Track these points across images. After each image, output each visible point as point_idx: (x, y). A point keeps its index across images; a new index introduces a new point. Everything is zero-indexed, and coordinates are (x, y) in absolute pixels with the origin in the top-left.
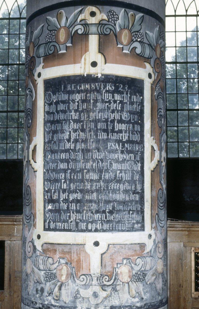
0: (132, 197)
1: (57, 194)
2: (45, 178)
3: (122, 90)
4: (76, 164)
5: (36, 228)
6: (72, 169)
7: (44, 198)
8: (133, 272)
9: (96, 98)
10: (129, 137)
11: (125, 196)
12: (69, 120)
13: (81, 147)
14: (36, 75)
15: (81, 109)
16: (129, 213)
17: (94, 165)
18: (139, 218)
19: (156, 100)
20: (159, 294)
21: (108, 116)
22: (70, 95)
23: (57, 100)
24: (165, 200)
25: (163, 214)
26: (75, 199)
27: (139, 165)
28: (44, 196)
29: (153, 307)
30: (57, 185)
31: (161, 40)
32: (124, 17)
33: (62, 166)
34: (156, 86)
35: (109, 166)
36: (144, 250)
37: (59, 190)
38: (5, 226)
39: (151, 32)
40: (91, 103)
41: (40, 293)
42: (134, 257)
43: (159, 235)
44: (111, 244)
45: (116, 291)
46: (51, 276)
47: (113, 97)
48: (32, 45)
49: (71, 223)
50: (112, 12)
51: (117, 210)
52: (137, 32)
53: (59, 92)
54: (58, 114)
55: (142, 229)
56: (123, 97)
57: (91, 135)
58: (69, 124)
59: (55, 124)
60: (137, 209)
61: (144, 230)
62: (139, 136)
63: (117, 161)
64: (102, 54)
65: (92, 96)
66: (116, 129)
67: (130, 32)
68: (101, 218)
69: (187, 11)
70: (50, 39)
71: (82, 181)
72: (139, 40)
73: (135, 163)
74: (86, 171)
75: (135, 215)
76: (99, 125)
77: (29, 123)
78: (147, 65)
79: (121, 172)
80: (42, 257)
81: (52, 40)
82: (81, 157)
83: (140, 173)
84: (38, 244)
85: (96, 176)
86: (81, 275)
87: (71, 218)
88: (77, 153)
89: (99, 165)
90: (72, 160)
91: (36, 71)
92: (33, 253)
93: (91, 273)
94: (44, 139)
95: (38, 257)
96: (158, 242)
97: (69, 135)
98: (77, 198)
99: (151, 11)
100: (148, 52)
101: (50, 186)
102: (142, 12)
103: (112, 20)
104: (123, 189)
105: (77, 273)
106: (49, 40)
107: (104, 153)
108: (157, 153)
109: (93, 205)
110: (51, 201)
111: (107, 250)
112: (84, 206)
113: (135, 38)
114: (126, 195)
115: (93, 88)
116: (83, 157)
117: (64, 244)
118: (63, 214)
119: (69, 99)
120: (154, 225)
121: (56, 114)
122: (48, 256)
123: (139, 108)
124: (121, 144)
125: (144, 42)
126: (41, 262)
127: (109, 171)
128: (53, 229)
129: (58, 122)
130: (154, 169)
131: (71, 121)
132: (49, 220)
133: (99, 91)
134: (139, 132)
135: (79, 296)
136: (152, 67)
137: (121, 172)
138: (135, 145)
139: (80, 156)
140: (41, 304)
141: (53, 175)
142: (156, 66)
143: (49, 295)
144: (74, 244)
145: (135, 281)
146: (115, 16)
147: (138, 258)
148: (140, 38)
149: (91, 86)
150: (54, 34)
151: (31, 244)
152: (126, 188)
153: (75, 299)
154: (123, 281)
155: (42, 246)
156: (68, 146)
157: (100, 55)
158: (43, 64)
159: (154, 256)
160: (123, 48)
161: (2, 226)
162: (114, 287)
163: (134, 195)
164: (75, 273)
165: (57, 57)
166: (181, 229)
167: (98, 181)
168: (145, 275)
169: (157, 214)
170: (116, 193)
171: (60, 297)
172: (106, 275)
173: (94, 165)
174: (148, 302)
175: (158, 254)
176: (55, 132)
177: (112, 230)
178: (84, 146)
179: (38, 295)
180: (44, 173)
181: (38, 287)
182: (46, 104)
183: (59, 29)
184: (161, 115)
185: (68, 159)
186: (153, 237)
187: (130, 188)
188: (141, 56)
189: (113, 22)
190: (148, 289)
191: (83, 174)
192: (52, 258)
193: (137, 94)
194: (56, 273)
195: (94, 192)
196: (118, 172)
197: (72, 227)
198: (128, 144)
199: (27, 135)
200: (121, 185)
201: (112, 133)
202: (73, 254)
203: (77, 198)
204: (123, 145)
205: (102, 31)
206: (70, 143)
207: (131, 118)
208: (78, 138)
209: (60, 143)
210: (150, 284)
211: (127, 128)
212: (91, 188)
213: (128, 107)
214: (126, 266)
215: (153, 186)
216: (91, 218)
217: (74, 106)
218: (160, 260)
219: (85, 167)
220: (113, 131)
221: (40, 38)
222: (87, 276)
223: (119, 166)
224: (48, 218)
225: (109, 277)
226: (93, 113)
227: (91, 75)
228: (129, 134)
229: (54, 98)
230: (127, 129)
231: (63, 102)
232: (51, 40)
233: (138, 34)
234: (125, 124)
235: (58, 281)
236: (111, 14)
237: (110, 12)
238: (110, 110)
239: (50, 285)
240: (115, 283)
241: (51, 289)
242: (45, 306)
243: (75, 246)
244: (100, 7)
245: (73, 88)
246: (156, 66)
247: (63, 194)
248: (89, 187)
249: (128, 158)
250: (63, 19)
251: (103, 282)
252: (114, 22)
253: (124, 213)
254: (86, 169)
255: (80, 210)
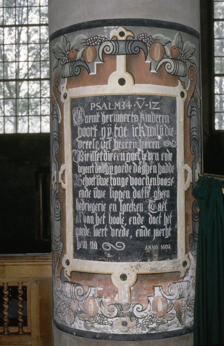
84: (68, 269)
130: (187, 189)
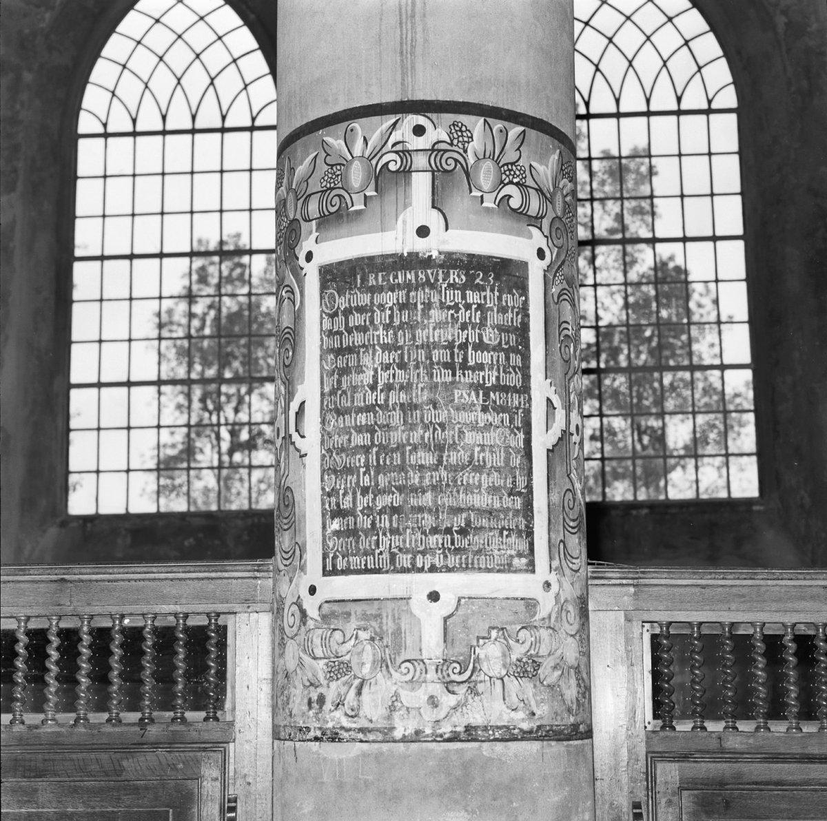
0: (508, 502)
1: (349, 498)
2: (325, 466)
3: (482, 283)
4: (390, 435)
5: (305, 574)
6: (380, 445)
7: (324, 509)
8: (512, 656)
9: (429, 299)
10: (498, 378)
11: (492, 499)
12: (374, 345)
13: (399, 399)
14: (302, 256)
15: (398, 323)
16: (501, 534)
17: (427, 435)
18: (523, 546)
19: (557, 303)
20: (569, 710)
21: (453, 335)
22: (375, 295)
23: (348, 306)
24: (580, 515)
25: (577, 544)
26: (387, 505)
27: (521, 436)
28: (323, 504)
29: (556, 735)
30: (351, 480)
31: (565, 180)
32: (485, 136)
33: (359, 440)
34: (555, 276)
35: (456, 438)
36: (535, 613)
37: (354, 490)
38: (234, 581)
39: (541, 164)
40: (417, 310)
41: (318, 707)
42: (513, 626)
43: (567, 585)
44: (464, 598)
45: (477, 694)
46: (339, 669)
47: (464, 297)
48: (291, 197)
49: (380, 556)
50: (458, 126)
51: (476, 528)
52: (512, 164)
53: (351, 289)
54: (349, 334)
55: (530, 568)
56: (485, 297)
57: (418, 374)
58: (374, 354)
59: (343, 356)
60: (517, 526)
61: (533, 571)
62: (520, 376)
63: (474, 427)
64: (440, 210)
65: (419, 297)
66: (471, 363)
67: (496, 166)
68: (443, 544)
69: (679, 99)
70: (330, 183)
71: (402, 468)
72: (515, 180)
73: (512, 431)
74: (410, 448)
75: (513, 539)
76: (436, 356)
77: (287, 358)
78: (534, 231)
79: (483, 451)
80: (320, 632)
81: (335, 185)
82: (400, 420)
83: (523, 453)
84: (311, 606)
85: (431, 457)
86: (403, 662)
87: (381, 546)
88: (390, 411)
89: (436, 436)
90: (379, 428)
91: (301, 249)
92: (300, 626)
93: (423, 657)
94: (322, 388)
95: (312, 632)
96: (566, 601)
97: (374, 376)
98: (392, 503)
99: (541, 121)
100: (534, 206)
101: (336, 483)
102: (522, 124)
103: (458, 142)
104: (487, 485)
105: (395, 658)
106: (328, 185)
107: (446, 412)
108: (560, 414)
109: (426, 518)
110: (338, 513)
111: (457, 609)
112: (408, 519)
113: (508, 176)
114: (495, 497)
115: (422, 279)
116: (404, 421)
117: (367, 600)
118: (363, 537)
119: (372, 302)
120: (556, 563)
121: (347, 334)
122: (332, 627)
123: (519, 320)
124: (481, 392)
125: (527, 184)
126: (317, 641)
127: (459, 448)
128: (342, 570)
129: (351, 350)
130: (553, 446)
131: (377, 347)
132: (335, 553)
133: (432, 286)
134: (519, 368)
135: (400, 704)
136: (546, 237)
137: (483, 451)
138: (512, 396)
139: (396, 417)
140: (320, 728)
141: (340, 460)
142: (554, 234)
143: (336, 709)
144: (388, 599)
145: (516, 675)
146: (465, 134)
147: (523, 628)
148: (518, 176)
149: (417, 276)
150: (338, 173)
151: (295, 608)
152: (493, 483)
153: (391, 711)
154: (490, 675)
155: (320, 607)
156: (371, 398)
157: (435, 212)
158: (318, 234)
159: (556, 628)
160: (482, 197)
161: (230, 581)
162: (472, 685)
163: (512, 497)
164: (390, 659)
165: (345, 219)
166: (618, 582)
167: (435, 468)
168: (537, 666)
169: (561, 541)
170: (472, 493)
171: (358, 709)
172: (454, 661)
173: (427, 435)
174: (544, 722)
175: (566, 625)
176: (345, 371)
177: (466, 568)
178: (405, 397)
179: (311, 713)
180: (323, 456)
181: (311, 695)
182: (324, 316)
183: (350, 163)
184: (567, 336)
185: (372, 425)
186: (555, 587)
187: (502, 485)
188: (521, 213)
189: (460, 145)
190: (545, 696)
191: (403, 454)
192: (341, 630)
193: (514, 291)
194: (350, 662)
195: (427, 492)
196: (477, 449)
197: (383, 564)
198: (497, 393)
199: (284, 383)
200: (484, 476)
201: (463, 371)
202: (385, 618)
203: (392, 503)
204: (486, 395)
205: (438, 164)
206: (375, 393)
207: (501, 339)
208: (391, 381)
209: (355, 393)
210: (549, 686)
211: (495, 360)
212: (421, 482)
213: (494, 318)
214: (497, 643)
215: (552, 482)
216: (421, 544)
217: (383, 317)
218: (570, 640)
219: (408, 440)
220: (464, 366)
221: (309, 181)
222: (416, 664)
223: (479, 438)
224: (332, 550)
225: (461, 666)
226: (423, 330)
227: (417, 254)
228: (499, 373)
229: (342, 303)
230: (495, 363)
231: (361, 310)
232: (332, 185)
233: (514, 168)
234: (489, 352)
235: (355, 677)
236: (457, 129)
237: (454, 125)
238: (457, 323)
239: (338, 687)
240: (473, 678)
241: (339, 694)
242: (328, 732)
243: (389, 602)
244: (434, 116)
245: (380, 279)
246: (554, 234)
247: (364, 496)
248: (417, 481)
249: (497, 422)
250: (358, 141)
251: (448, 675)
252: (464, 145)
253: (491, 534)
254: (410, 445)
255: (398, 528)
